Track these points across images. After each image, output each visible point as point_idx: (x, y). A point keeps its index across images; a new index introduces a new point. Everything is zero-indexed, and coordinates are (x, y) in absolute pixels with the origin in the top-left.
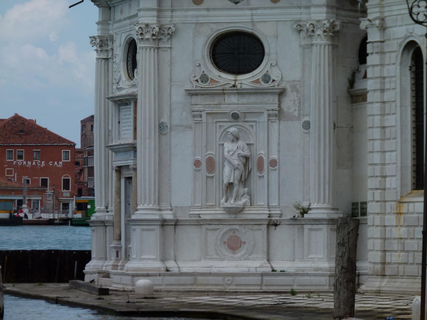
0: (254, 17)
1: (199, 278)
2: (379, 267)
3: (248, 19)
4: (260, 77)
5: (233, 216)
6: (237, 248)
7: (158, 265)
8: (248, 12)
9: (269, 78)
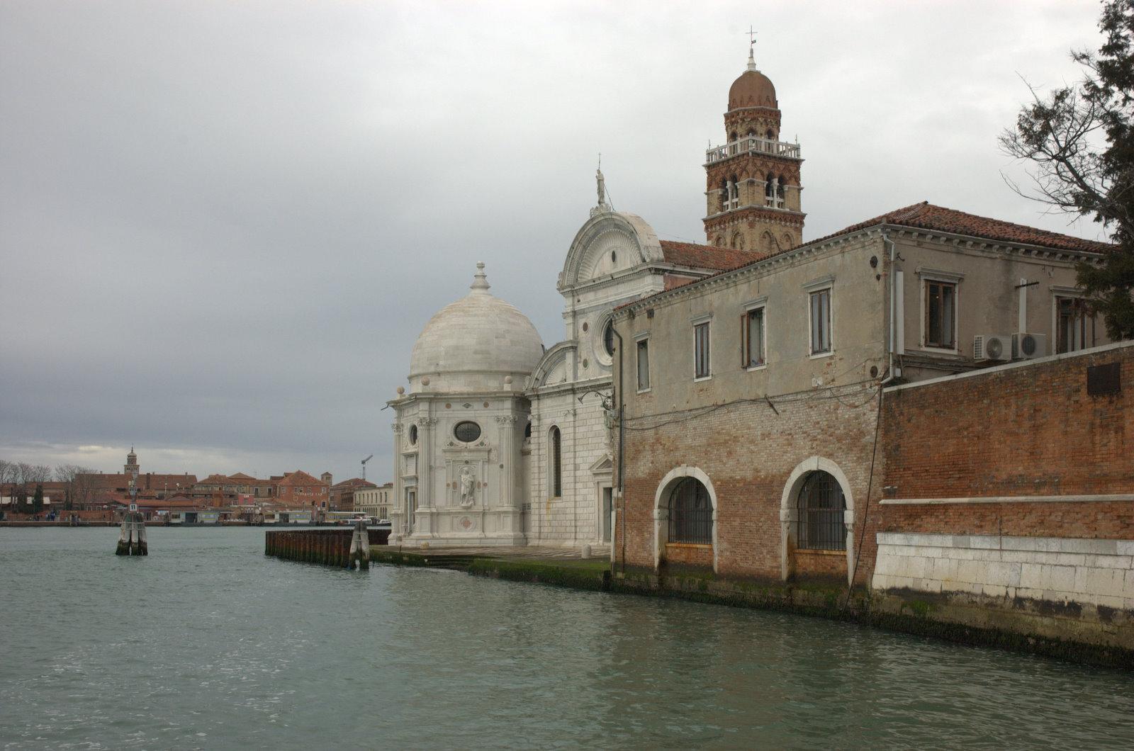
1: (450, 540)
2: (537, 535)
5: (465, 511)
7: (429, 534)
8: (473, 412)
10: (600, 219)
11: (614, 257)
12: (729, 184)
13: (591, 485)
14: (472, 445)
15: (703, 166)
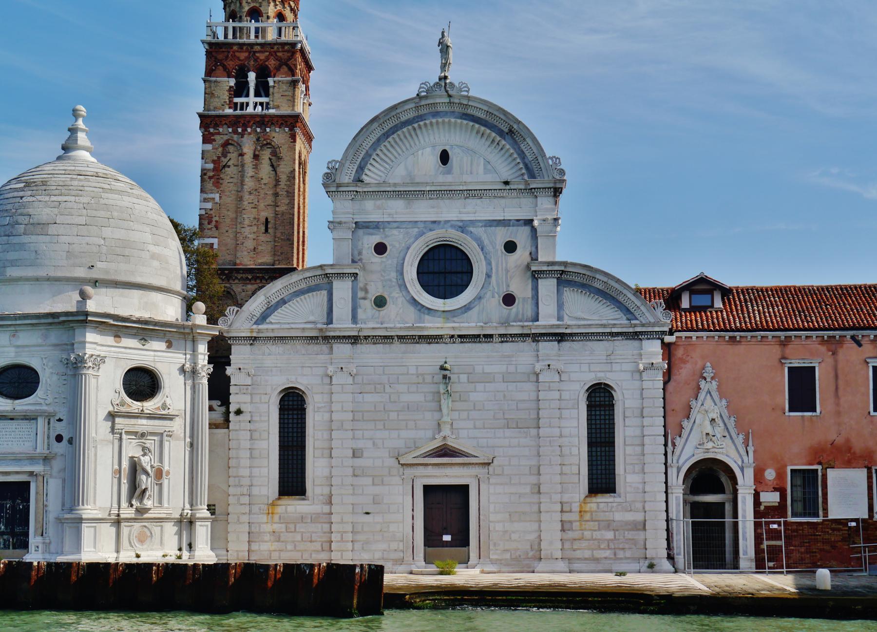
0: (156, 358)
3: (151, 359)
4: (160, 405)
6: (144, 541)
8: (152, 353)
9: (166, 406)
10: (438, 101)
11: (445, 157)
12: (252, 76)
13: (397, 480)
14: (150, 406)
15: (203, 42)
